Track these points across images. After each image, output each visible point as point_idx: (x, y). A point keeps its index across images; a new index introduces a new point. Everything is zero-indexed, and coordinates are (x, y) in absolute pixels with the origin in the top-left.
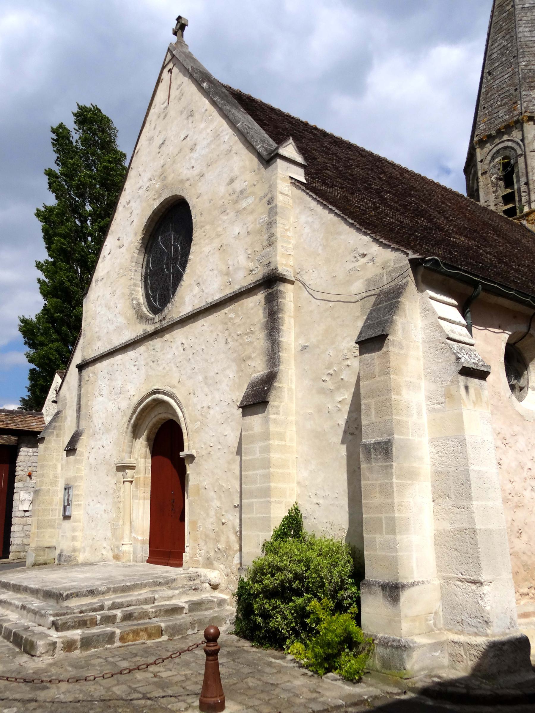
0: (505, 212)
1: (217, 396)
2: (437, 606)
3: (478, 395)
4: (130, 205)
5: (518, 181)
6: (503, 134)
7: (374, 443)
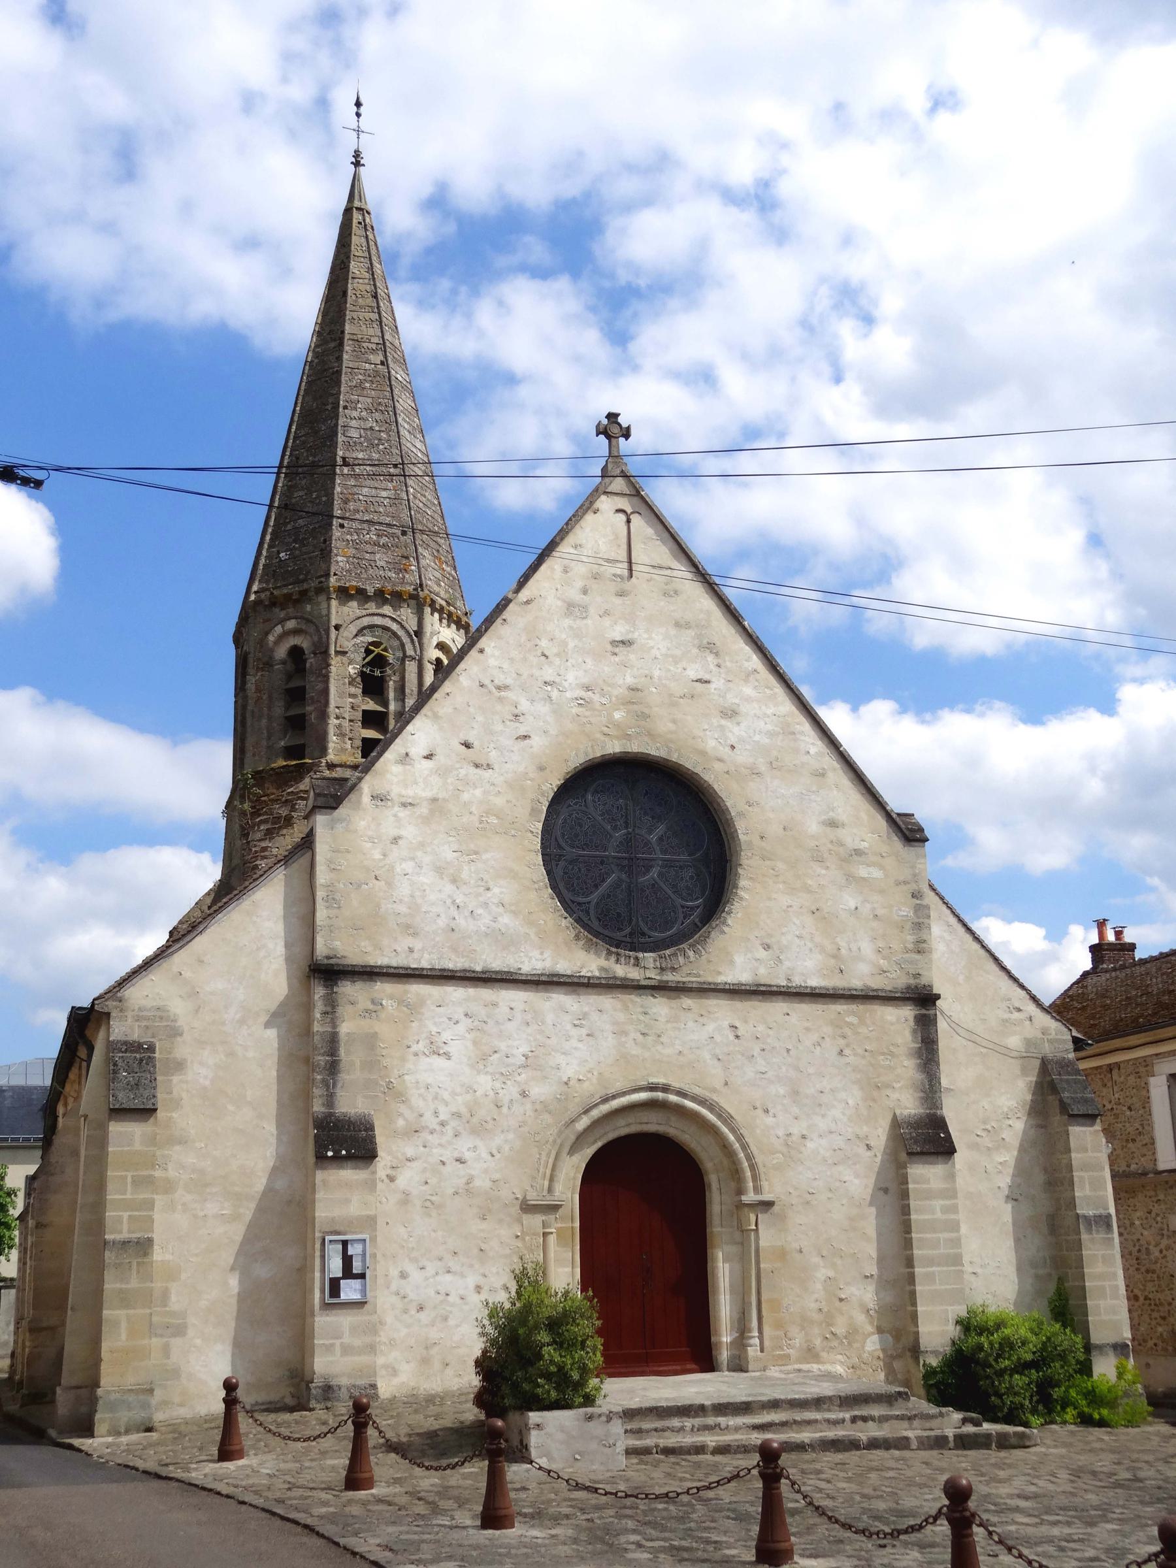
1: (822, 1124)
6: (385, 601)
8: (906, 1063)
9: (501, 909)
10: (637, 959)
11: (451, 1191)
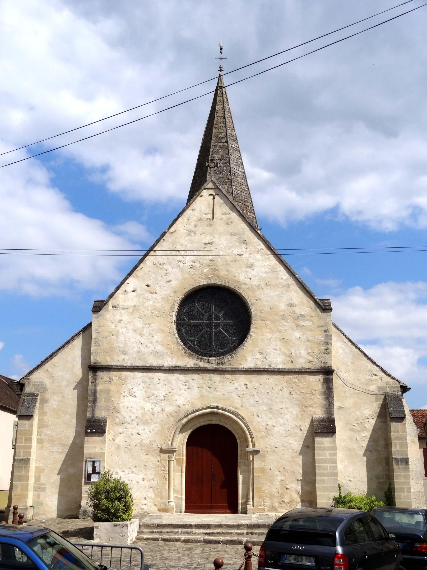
1: (281, 421)
7: (401, 459)
8: (319, 397)
9: (157, 343)
10: (208, 360)
11: (135, 444)
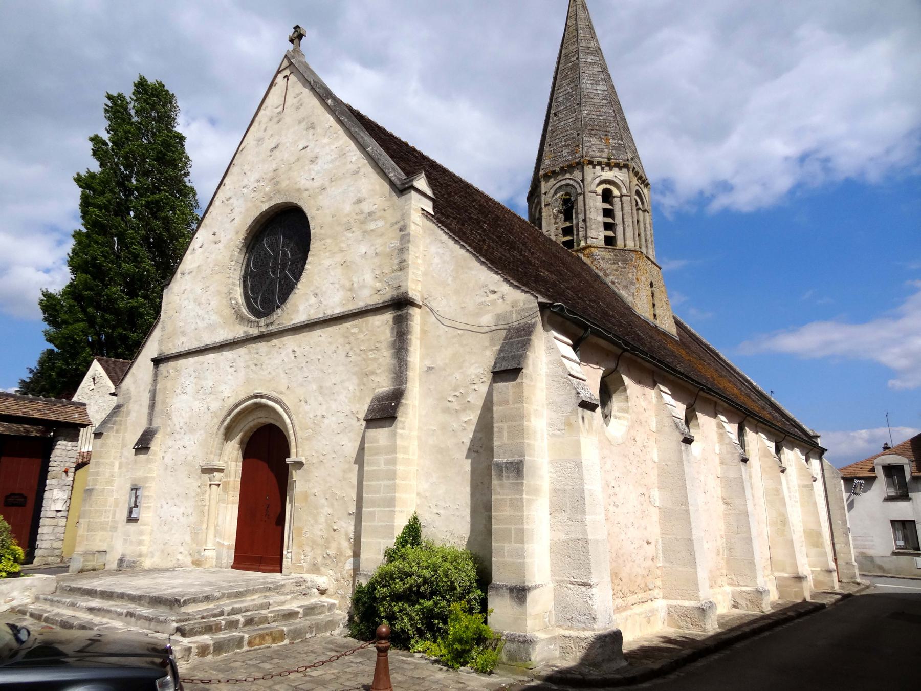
0: (564, 243)
1: (334, 406)
2: (551, 606)
3: (590, 424)
4: (231, 201)
5: (577, 217)
6: (566, 172)
7: (506, 463)
8: (386, 354)
